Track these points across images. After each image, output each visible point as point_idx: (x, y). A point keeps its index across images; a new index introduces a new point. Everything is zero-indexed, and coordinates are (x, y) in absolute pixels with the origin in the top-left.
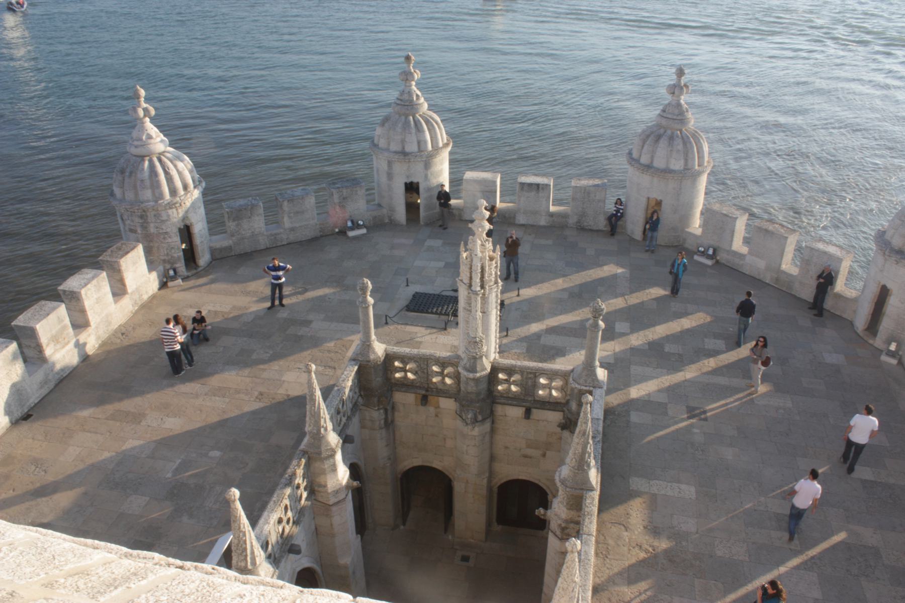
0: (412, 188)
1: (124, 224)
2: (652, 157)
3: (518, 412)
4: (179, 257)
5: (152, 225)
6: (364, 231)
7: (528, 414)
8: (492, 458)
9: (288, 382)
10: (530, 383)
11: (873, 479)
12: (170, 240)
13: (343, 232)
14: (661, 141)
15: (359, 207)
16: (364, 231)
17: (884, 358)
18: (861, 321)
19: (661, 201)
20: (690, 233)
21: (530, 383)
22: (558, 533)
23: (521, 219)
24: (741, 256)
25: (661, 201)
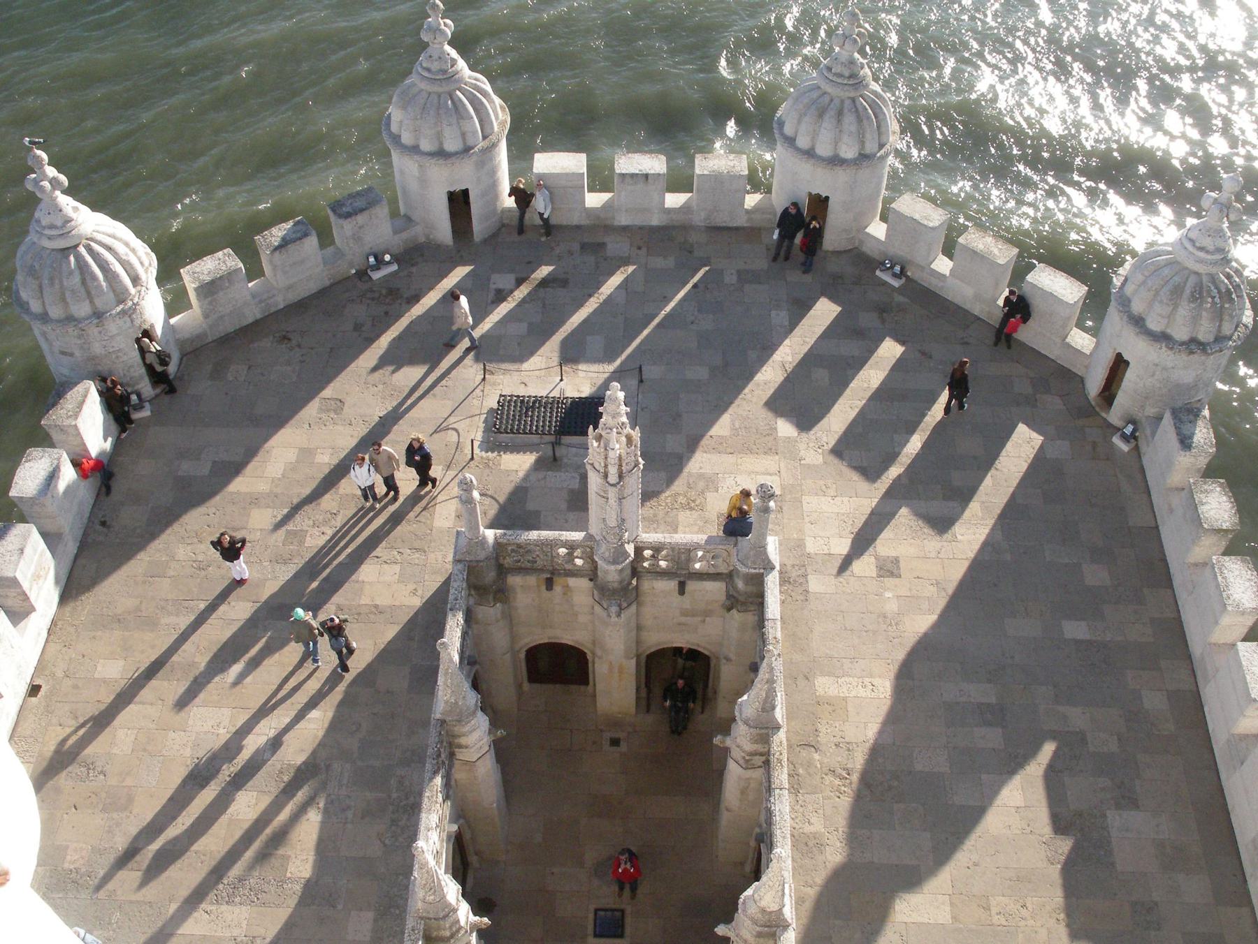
0: (459, 202)
1: (51, 345)
2: (813, 139)
3: (672, 585)
4: (141, 378)
5: (97, 345)
6: (395, 267)
7: (682, 589)
8: (639, 628)
9: (370, 583)
10: (683, 557)
11: (1088, 637)
12: (125, 358)
13: (362, 274)
14: (827, 117)
15: (377, 230)
16: (395, 267)
17: (1116, 440)
18: (1094, 385)
19: (827, 198)
20: (868, 234)
21: (683, 557)
22: (741, 762)
23: (623, 220)
24: (941, 276)
25: (827, 198)
